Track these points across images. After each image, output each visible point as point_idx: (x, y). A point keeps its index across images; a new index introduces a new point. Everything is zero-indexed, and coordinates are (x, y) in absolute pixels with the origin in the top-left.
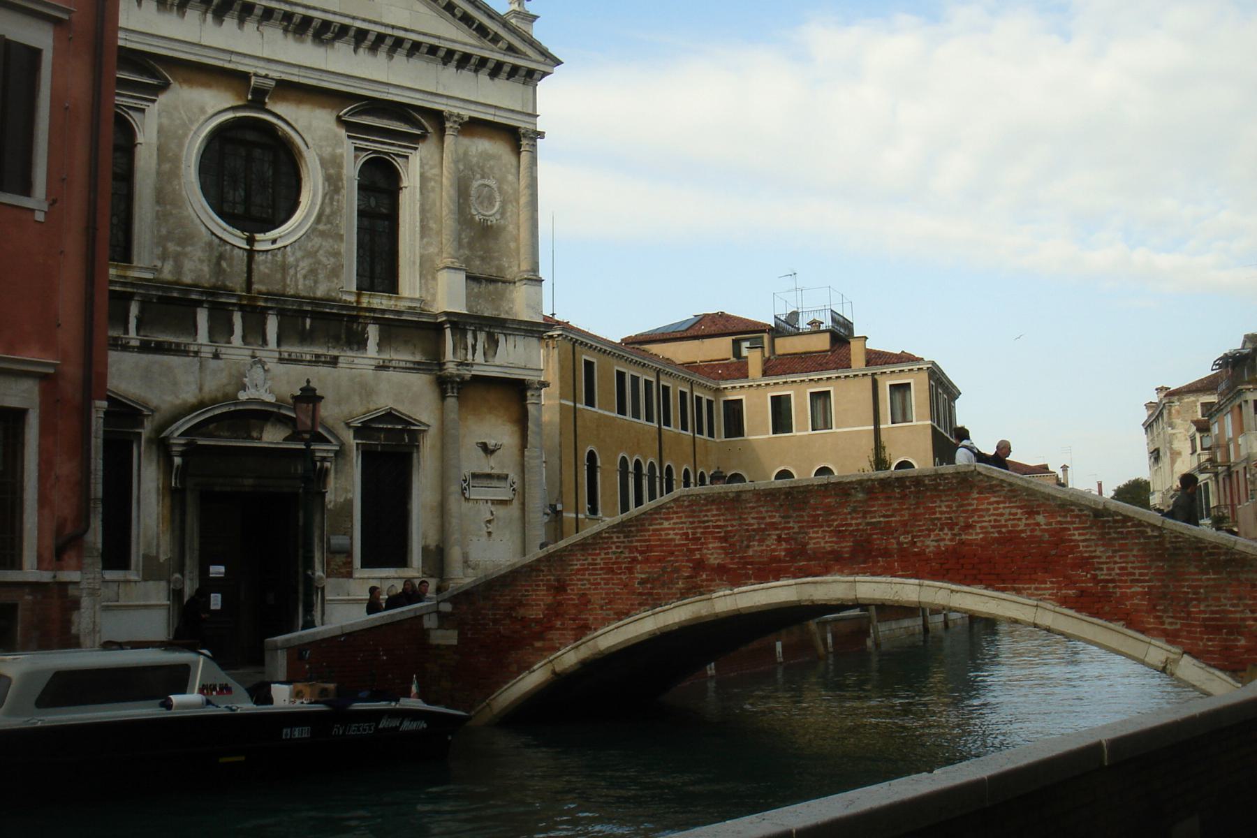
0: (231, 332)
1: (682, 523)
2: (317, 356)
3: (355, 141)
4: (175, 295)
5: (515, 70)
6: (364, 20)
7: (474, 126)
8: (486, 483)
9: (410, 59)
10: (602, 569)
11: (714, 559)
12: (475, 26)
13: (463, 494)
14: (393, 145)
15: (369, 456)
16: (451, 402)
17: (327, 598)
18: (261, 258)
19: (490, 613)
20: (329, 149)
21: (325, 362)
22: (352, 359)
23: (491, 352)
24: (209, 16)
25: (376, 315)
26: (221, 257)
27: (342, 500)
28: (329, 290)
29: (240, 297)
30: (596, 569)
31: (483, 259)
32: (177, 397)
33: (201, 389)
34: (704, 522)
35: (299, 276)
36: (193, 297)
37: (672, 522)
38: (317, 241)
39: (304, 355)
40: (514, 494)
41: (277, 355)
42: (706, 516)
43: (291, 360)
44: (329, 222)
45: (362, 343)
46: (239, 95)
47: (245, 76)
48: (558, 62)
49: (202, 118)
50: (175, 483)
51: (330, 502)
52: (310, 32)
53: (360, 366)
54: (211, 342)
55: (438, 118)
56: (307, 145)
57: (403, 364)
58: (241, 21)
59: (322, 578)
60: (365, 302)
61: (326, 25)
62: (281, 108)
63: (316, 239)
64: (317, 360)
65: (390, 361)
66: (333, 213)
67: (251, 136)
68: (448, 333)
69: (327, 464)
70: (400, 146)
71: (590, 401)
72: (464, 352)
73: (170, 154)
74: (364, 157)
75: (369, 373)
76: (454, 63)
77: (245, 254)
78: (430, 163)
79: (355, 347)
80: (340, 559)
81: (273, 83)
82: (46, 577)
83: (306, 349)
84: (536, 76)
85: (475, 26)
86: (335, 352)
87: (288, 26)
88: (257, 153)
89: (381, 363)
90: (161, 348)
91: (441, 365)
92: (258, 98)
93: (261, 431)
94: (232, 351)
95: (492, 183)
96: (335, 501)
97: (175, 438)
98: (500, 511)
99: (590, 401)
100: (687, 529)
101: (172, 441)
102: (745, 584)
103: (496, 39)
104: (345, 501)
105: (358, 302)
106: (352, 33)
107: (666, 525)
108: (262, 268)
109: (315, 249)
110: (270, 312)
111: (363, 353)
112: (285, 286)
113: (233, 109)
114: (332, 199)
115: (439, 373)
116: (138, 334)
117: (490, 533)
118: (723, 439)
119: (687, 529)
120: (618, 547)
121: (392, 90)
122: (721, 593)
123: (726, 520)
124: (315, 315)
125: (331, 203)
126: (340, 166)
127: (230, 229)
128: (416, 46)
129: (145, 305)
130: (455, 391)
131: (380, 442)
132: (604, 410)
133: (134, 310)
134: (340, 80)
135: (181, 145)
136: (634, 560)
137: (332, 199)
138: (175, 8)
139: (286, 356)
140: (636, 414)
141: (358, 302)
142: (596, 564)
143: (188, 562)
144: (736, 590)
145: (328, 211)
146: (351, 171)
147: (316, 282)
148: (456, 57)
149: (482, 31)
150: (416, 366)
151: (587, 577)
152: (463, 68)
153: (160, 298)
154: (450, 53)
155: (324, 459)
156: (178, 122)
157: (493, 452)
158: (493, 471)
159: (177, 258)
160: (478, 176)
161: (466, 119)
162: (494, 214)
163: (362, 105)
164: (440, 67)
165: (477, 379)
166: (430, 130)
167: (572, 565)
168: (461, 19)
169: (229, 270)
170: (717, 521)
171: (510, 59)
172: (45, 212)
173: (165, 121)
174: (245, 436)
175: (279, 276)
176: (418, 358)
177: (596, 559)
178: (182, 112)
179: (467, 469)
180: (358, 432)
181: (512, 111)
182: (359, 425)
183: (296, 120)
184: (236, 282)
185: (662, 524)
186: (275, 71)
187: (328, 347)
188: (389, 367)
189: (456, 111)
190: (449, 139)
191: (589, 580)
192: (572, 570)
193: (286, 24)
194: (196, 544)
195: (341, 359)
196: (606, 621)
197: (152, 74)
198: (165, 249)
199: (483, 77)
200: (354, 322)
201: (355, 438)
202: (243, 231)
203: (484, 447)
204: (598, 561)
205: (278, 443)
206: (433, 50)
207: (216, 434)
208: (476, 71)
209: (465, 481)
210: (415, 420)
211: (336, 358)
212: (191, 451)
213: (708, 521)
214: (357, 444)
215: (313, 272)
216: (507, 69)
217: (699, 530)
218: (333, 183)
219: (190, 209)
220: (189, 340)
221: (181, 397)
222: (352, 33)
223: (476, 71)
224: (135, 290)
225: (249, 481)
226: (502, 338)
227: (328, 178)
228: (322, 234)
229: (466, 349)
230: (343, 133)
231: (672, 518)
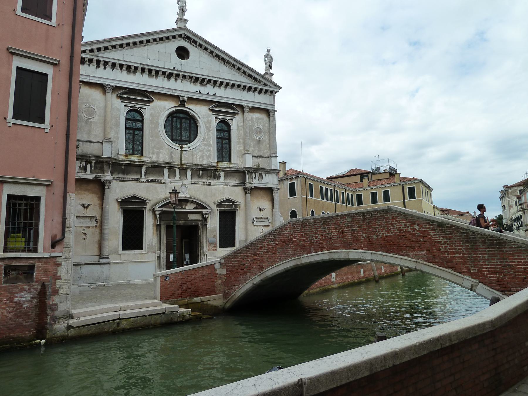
0: (175, 176)
1: (291, 231)
2: (204, 182)
3: (215, 116)
4: (157, 165)
5: (266, 91)
6: (216, 77)
7: (253, 109)
8: (260, 220)
9: (232, 89)
10: (267, 248)
11: (302, 243)
12: (253, 78)
13: (253, 224)
14: (228, 116)
15: (222, 214)
16: (248, 195)
17: (208, 257)
18: (185, 153)
19: (235, 263)
20: (206, 119)
21: (206, 184)
22: (215, 183)
23: (260, 179)
24: (166, 79)
25: (223, 169)
26: (172, 153)
27: (213, 227)
28: (207, 162)
29: (178, 165)
30: (265, 248)
31: (258, 150)
32: (158, 197)
33: (166, 194)
34: (298, 230)
36: (163, 165)
37: (288, 231)
38: (203, 147)
39: (199, 182)
40: (270, 224)
41: (191, 182)
42: (298, 228)
43: (195, 184)
45: (218, 178)
46: (176, 103)
47: (178, 97)
48: (280, 88)
49: (165, 110)
50: (158, 223)
51: (209, 227)
52: (199, 82)
53: (218, 185)
54: (169, 179)
55: (242, 107)
56: (199, 117)
58: (176, 80)
59: (206, 251)
60: (219, 165)
61: (203, 80)
62: (190, 106)
63: (203, 146)
64: (204, 184)
65: (228, 183)
66: (208, 138)
67: (181, 115)
68: (247, 174)
69: (207, 216)
70: (230, 117)
71: (311, 196)
72: (252, 179)
73: (155, 122)
74: (218, 121)
75: (221, 187)
76: (246, 90)
77: (180, 152)
78: (240, 121)
79: (217, 179)
80: (212, 245)
81: (187, 98)
82: (46, 255)
83: (200, 180)
84: (274, 93)
85: (253, 78)
86: (210, 181)
87: (191, 80)
88: (184, 120)
89: (225, 184)
90: (152, 181)
91: (245, 184)
92: (183, 104)
94: (176, 182)
95: (261, 127)
97: (157, 209)
99: (311, 196)
100: (292, 233)
101: (155, 210)
102: (311, 253)
103: (260, 82)
105: (217, 165)
106: (212, 82)
107: (286, 232)
108: (185, 156)
109: (203, 149)
110: (188, 169)
111: (219, 181)
112: (193, 161)
113: (175, 107)
114: (208, 134)
115: (244, 186)
116: (145, 177)
118: (356, 206)
119: (292, 233)
120: (271, 240)
121: (226, 99)
122: (304, 256)
123: (304, 230)
124: (204, 170)
126: (210, 123)
127: (175, 144)
128: (233, 85)
129: (147, 168)
130: (249, 191)
131: (225, 209)
132: (316, 198)
133: (144, 170)
135: (158, 119)
136: (276, 244)
137: (208, 134)
138: (154, 76)
140: (327, 199)
141: (217, 165)
142: (265, 246)
143: (162, 247)
144: (308, 255)
145: (207, 137)
146: (214, 125)
147: (203, 160)
148: (247, 88)
149: (255, 79)
150: (237, 184)
151: (262, 250)
152: (250, 91)
153: (152, 166)
154: (245, 87)
155: (206, 214)
156: (157, 112)
157: (263, 210)
159: (158, 154)
160: (256, 125)
161: (251, 107)
162: (261, 137)
163: (217, 104)
164: (242, 91)
165: (256, 188)
166: (239, 111)
167: (258, 246)
168: (248, 76)
169: (174, 157)
170: (302, 230)
171: (264, 88)
172: (49, 129)
173: (153, 112)
174: (181, 207)
175: (191, 158)
176: (237, 182)
177: (265, 244)
178: (158, 109)
179: (254, 217)
180: (218, 205)
181: (266, 104)
182: (218, 203)
183: (195, 110)
184: (178, 161)
185: (284, 232)
186: (187, 95)
187: (208, 180)
188: (228, 185)
189: (247, 105)
190: (246, 114)
191: (263, 252)
192: (258, 248)
193: (191, 80)
194: (165, 242)
195: (212, 183)
196: (268, 266)
197: (148, 97)
198: (153, 151)
199: (256, 94)
200: (216, 171)
201: (217, 207)
202: (179, 144)
203: (260, 209)
204: (266, 245)
206: (239, 86)
208: (254, 92)
209: (254, 220)
210: (236, 201)
212: (162, 213)
213: (299, 230)
215: (202, 156)
216: (264, 91)
217: (296, 234)
218: (209, 129)
219: (161, 138)
220: (161, 178)
221: (159, 196)
222: (212, 82)
223: (254, 92)
224: (143, 164)
226: (264, 175)
227: (207, 127)
228: (205, 145)
229: (252, 178)
230: (211, 113)
231: (288, 230)
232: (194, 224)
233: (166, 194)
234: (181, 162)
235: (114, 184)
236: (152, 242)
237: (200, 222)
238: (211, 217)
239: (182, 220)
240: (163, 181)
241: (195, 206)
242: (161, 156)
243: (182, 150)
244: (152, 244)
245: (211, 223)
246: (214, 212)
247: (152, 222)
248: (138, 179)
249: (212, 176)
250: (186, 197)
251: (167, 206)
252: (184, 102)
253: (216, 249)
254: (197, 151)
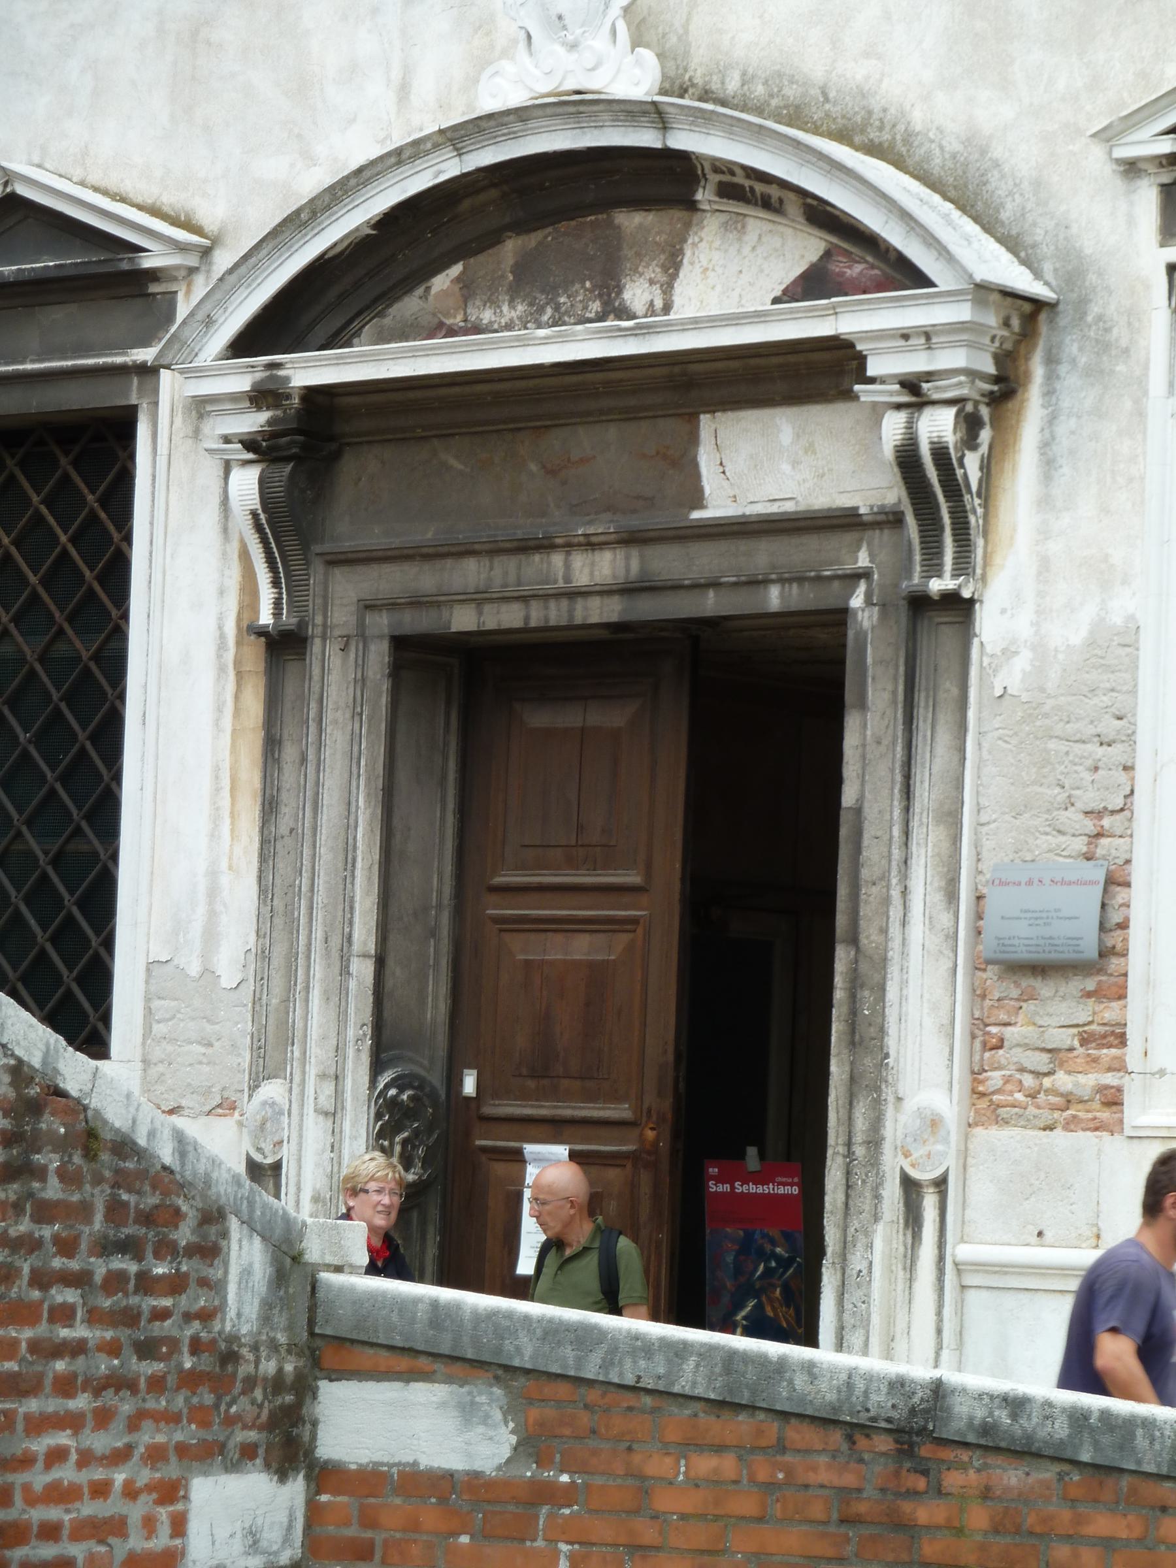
17: (962, 1251)
27: (1077, 637)
32: (310, 159)
33: (404, 91)
51: (1009, 653)
59: (935, 1123)
93: (673, 265)
96: (1040, 649)
97: (200, 373)
104: (1091, 643)
205: (758, 317)
207: (457, 320)
232: (775, 598)
233: (404, 91)
236: (211, 936)
237: (863, 560)
238: (1046, 445)
239: (590, 545)
244: (208, 972)
245: (1044, 565)
246: (1120, 333)
247: (222, 592)
251: (410, 306)
253: (1113, 1100)
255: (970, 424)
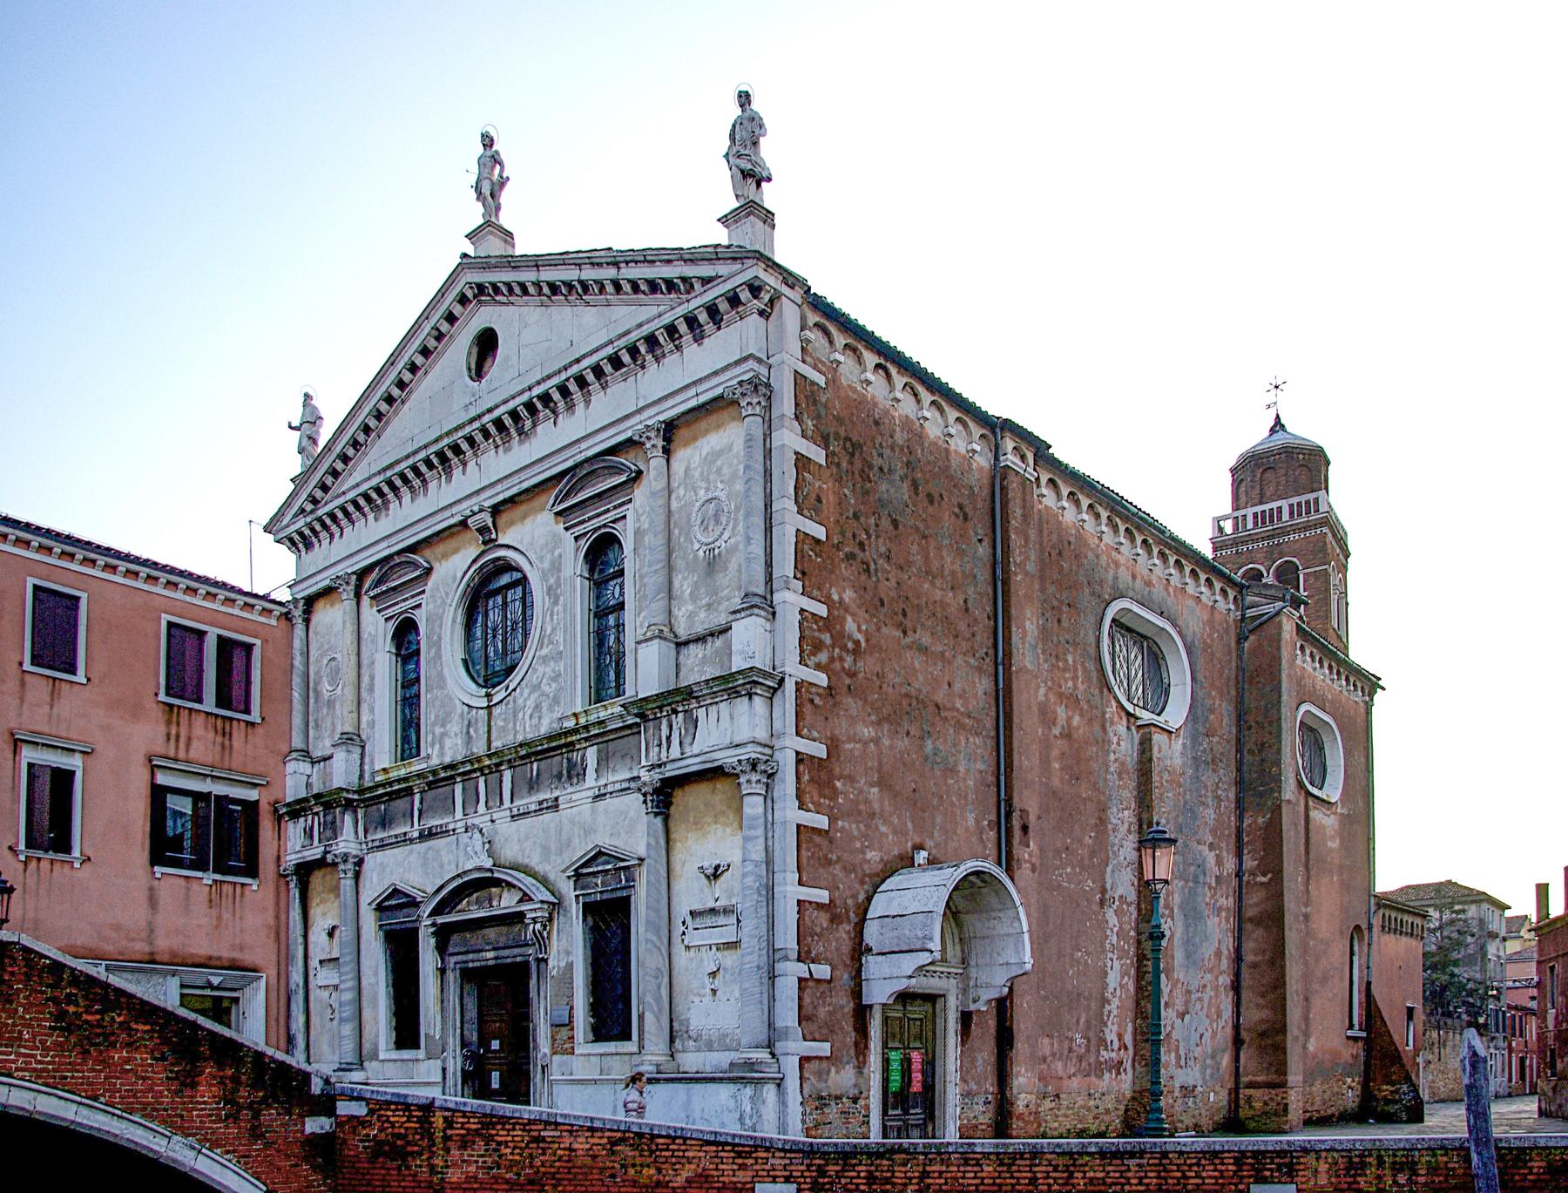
2: (541, 803)
8: (709, 921)
20: (549, 556)
21: (547, 808)
35: (527, 717)
38: (541, 669)
44: (551, 642)
57: (618, 786)
66: (554, 630)
72: (657, 749)
86: (555, 795)
98: (729, 959)
113: (474, 561)
114: (552, 616)
117: (714, 991)
125: (552, 619)
131: (598, 889)
134: (537, 469)
139: (515, 812)
147: (540, 718)
158: (718, 904)
160: (702, 492)
175: (511, 725)
211: (557, 799)
214: (577, 896)
215: (538, 707)
220: (450, 819)
225: (490, 955)
226: (701, 713)
228: (545, 660)
234: (489, 749)
235: (372, 861)
240: (451, 827)
241: (519, 895)
242: (448, 743)
243: (489, 707)
248: (405, 834)
249: (565, 772)
250: (479, 869)
251: (459, 908)
252: (483, 530)
254: (526, 692)
255: (545, 927)
